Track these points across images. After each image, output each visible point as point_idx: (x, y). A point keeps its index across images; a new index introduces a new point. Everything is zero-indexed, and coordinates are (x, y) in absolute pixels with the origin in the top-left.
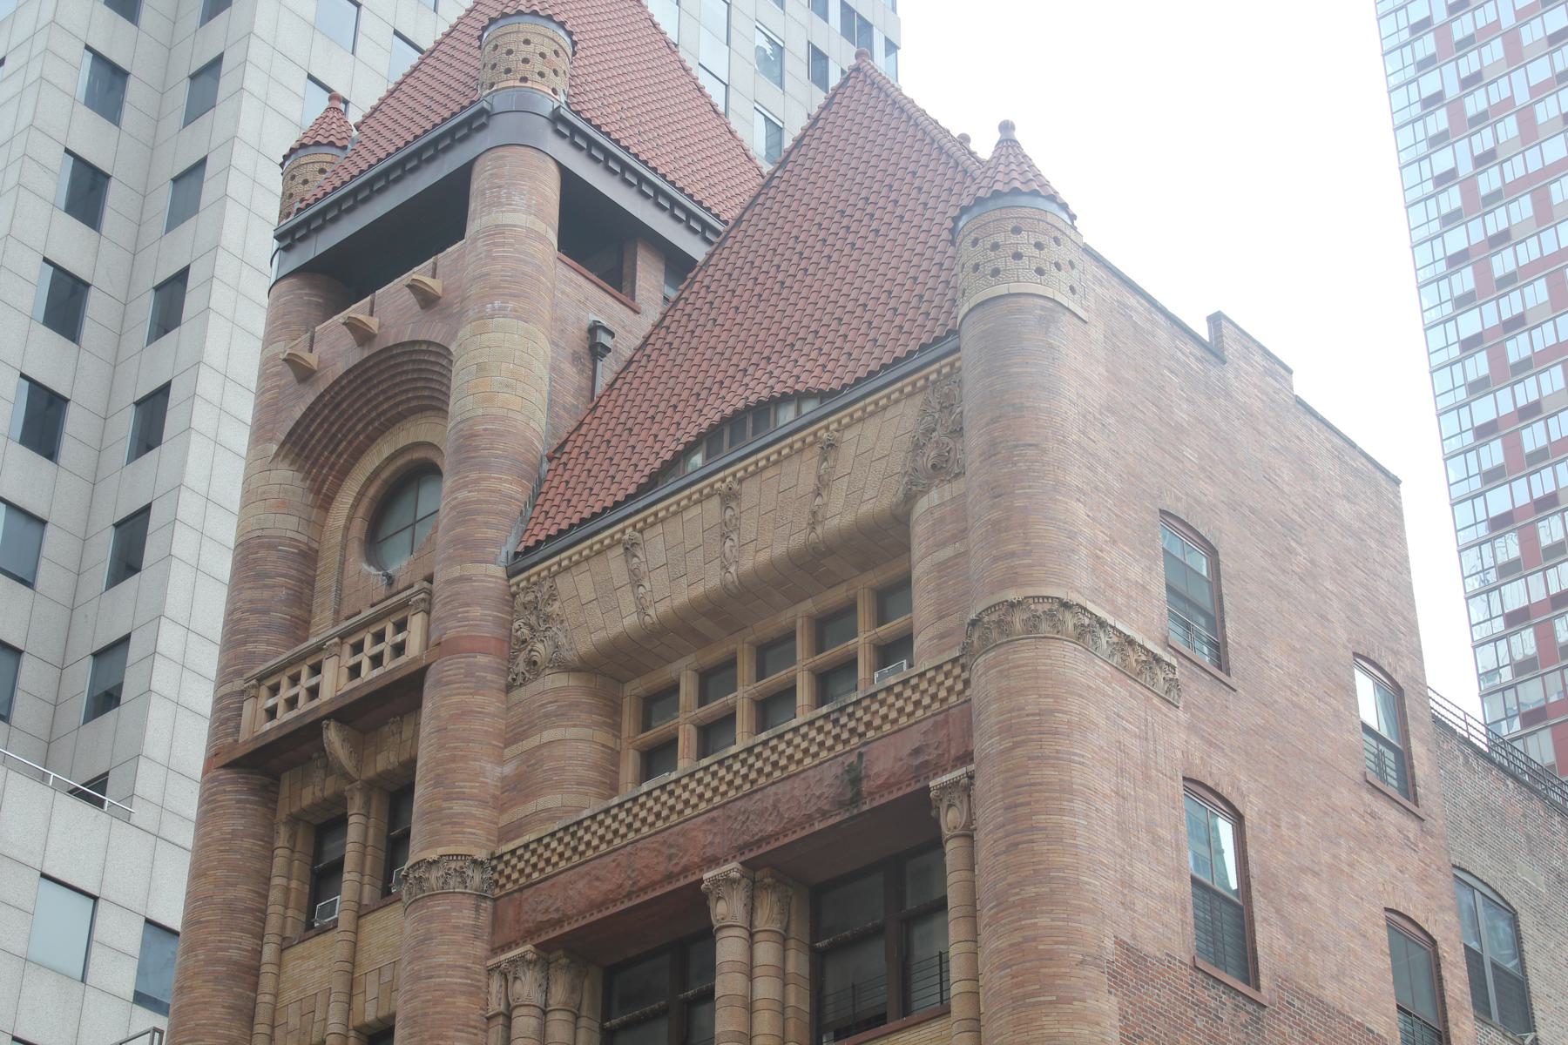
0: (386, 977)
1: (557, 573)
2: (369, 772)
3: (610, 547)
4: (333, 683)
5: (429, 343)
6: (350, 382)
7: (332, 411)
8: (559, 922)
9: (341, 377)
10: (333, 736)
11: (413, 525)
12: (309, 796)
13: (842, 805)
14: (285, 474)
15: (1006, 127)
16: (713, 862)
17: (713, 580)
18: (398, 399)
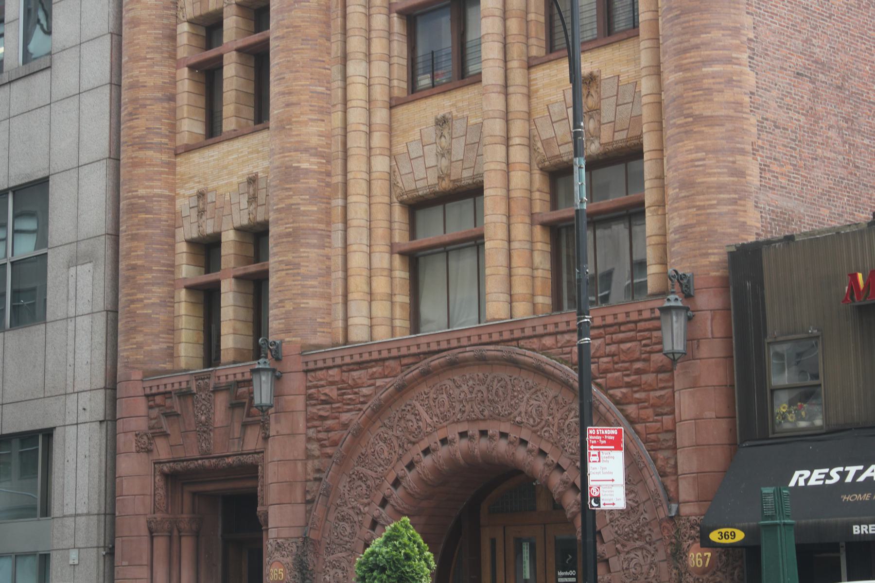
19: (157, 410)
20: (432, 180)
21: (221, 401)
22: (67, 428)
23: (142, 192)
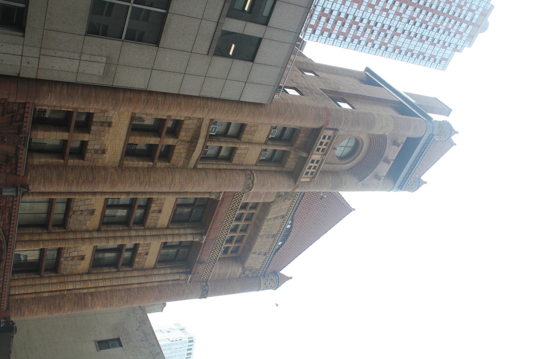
0: (243, 156)
4: (316, 156)
8: (220, 206)
10: (304, 155)
11: (345, 147)
13: (199, 260)
14: (381, 133)
15: (291, 278)
16: (207, 237)
17: (261, 234)
19: (17, 109)
20: (75, 208)
21: (10, 149)
22: (21, 47)
23: (122, 109)
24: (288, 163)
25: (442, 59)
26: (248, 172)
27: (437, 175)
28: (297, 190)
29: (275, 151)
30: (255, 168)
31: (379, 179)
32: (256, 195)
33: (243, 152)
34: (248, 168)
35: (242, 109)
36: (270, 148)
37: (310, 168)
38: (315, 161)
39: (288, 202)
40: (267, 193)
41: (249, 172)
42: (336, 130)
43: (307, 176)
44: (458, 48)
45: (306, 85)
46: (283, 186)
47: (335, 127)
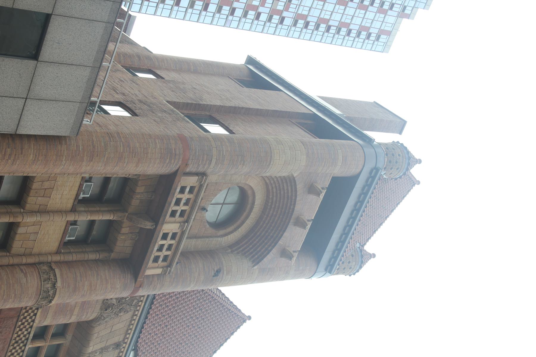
0: (32, 237)
1: (134, 312)
2: (124, 225)
3: (126, 336)
4: (170, 226)
5: (268, 253)
6: (290, 208)
7: (288, 196)
9: (294, 207)
10: (148, 225)
11: (223, 204)
12: (140, 189)
14: (284, 174)
18: (268, 218)
24: (119, 243)
25: (381, 32)
26: (44, 268)
27: (392, 239)
28: (141, 293)
29: (92, 223)
30: (57, 258)
31: (290, 257)
32: (63, 309)
33: (31, 229)
34: (42, 259)
35: (22, 149)
36: (83, 218)
37: (160, 249)
38: (170, 235)
39: (126, 317)
40: (84, 303)
41: (45, 268)
42: (202, 175)
43: (156, 265)
44: (406, 12)
45: (140, 97)
46: (113, 287)
47: (201, 169)
